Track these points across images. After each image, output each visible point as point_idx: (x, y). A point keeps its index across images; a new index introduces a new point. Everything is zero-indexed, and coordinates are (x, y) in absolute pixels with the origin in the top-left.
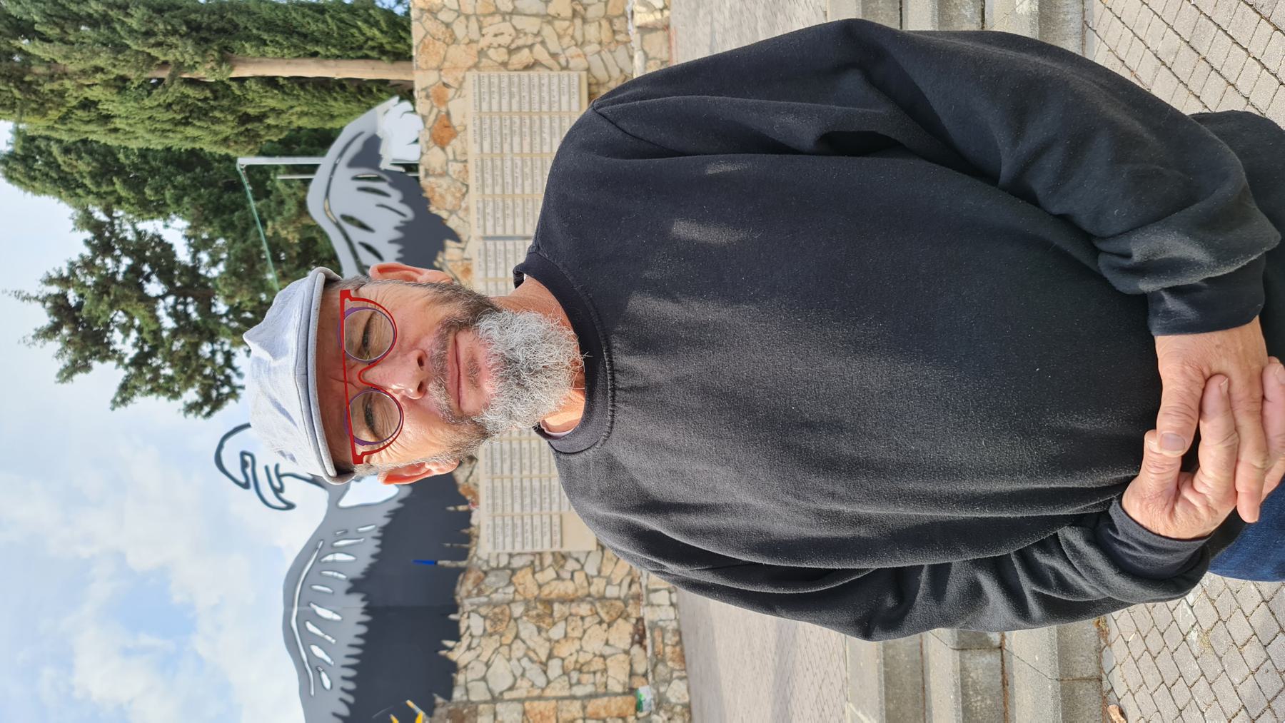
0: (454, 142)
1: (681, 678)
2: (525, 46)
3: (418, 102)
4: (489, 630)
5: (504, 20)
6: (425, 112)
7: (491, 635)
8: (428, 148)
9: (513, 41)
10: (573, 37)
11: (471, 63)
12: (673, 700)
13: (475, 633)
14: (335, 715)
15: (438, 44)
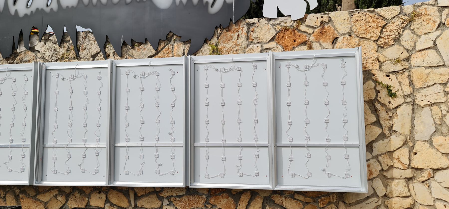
0: (280, 48)
3: (319, 15)
5: (405, 97)
6: (308, 22)
8: (273, 25)
9: (383, 105)
15: (378, 31)
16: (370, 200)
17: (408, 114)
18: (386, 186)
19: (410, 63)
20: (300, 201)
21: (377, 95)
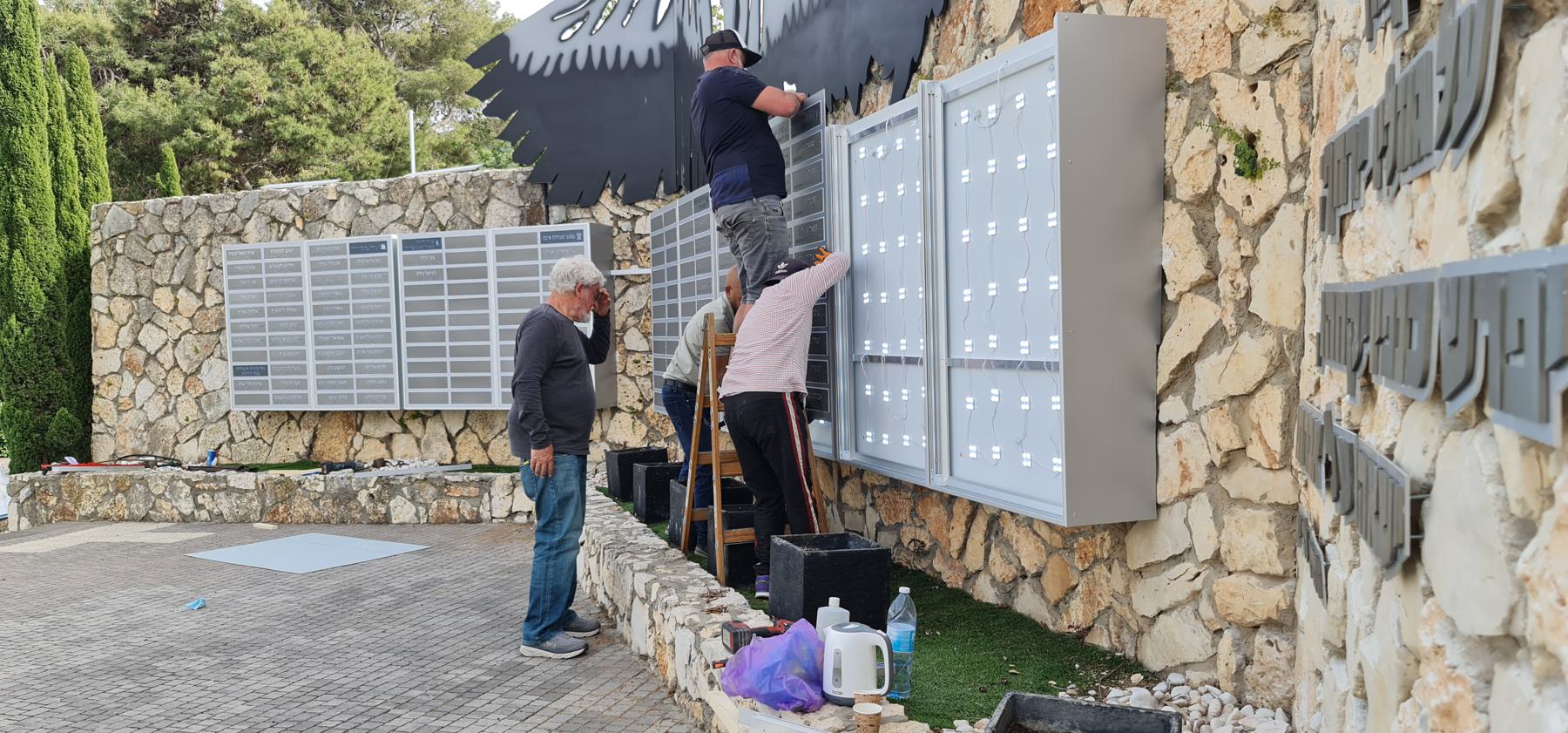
1: (417, 514)
2: (1212, 263)
4: (640, 243)
7: (633, 247)
9: (1231, 213)
10: (1233, 458)
11: (1180, 62)
12: (392, 504)
13: (638, 222)
14: (531, 56)
16: (1178, 569)
17: (1292, 244)
18: (1220, 526)
19: (1316, 17)
20: (1044, 542)
21: (1217, 176)
